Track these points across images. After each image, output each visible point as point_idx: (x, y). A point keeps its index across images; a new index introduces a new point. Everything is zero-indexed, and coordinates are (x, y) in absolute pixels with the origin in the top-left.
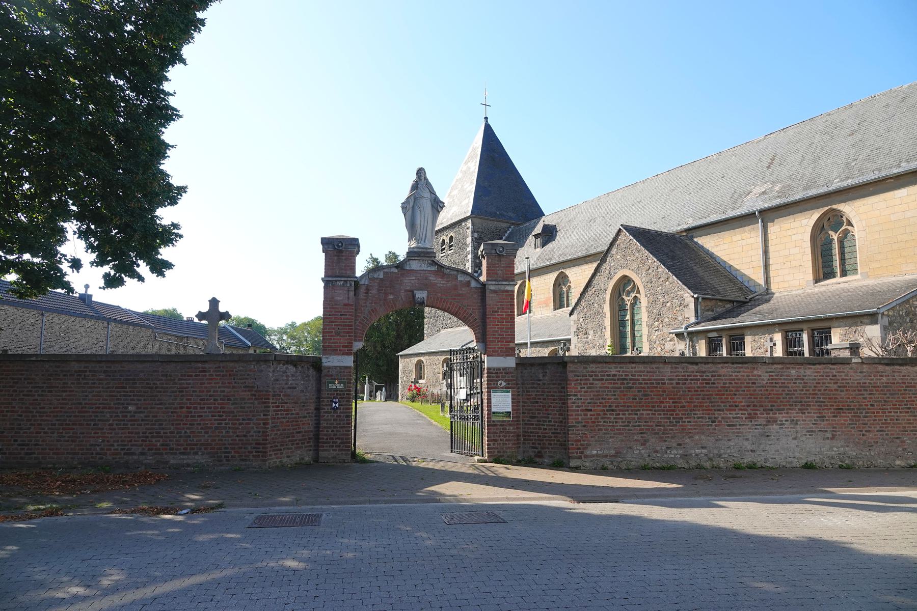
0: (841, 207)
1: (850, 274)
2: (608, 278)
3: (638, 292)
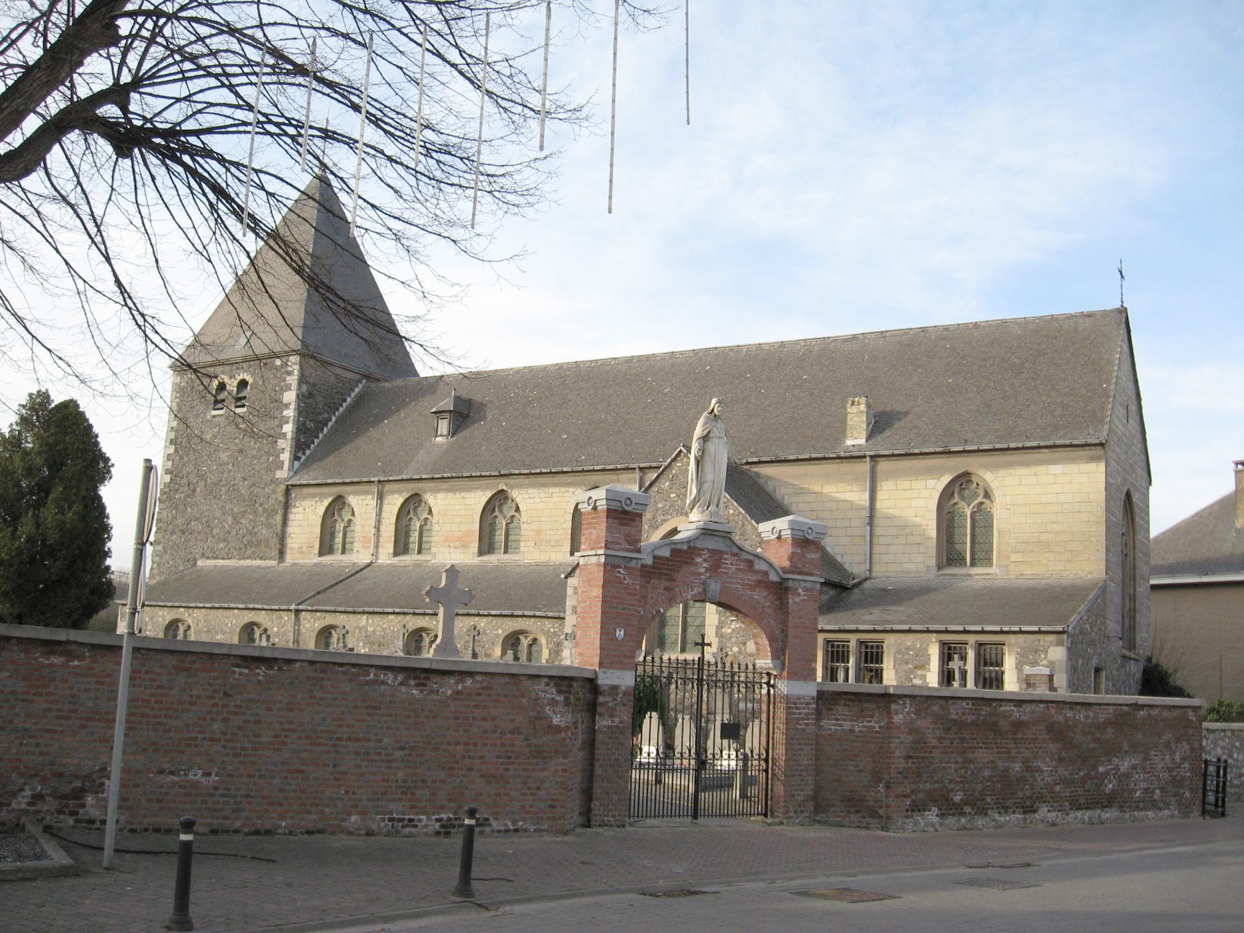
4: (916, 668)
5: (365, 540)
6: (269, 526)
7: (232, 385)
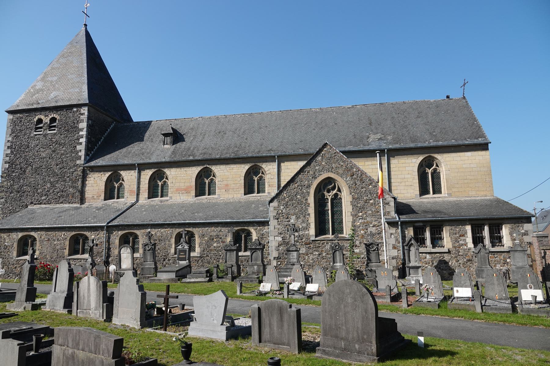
1: (437, 193)
2: (313, 177)
3: (339, 190)
4: (460, 236)
5: (131, 192)
6: (74, 187)
7: (46, 120)
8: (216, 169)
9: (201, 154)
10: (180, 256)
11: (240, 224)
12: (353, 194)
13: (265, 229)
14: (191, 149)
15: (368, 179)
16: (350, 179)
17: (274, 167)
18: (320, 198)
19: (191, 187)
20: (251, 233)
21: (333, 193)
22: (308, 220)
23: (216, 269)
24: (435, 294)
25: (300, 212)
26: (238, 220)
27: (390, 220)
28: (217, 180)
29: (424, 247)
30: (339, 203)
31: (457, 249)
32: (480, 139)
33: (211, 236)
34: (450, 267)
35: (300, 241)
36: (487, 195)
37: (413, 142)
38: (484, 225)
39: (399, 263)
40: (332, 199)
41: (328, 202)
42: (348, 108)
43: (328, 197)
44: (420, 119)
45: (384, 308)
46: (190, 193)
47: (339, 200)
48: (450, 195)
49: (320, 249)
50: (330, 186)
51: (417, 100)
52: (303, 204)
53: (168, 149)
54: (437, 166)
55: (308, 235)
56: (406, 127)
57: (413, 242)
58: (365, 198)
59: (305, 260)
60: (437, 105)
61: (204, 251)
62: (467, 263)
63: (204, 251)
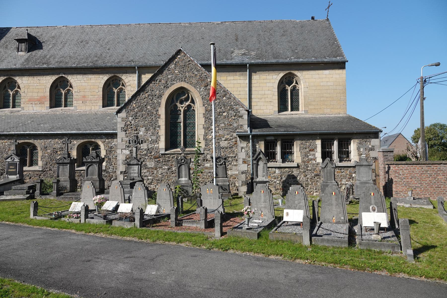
0: (296, 73)
1: (295, 110)
2: (164, 87)
3: (193, 102)
4: (310, 151)
8: (73, 79)
9: (57, 62)
10: (9, 170)
11: (87, 136)
12: (206, 105)
13: (114, 142)
14: (48, 57)
15: (222, 90)
16: (204, 90)
17: (134, 79)
18: (172, 110)
19: (45, 97)
20: (100, 146)
21: (186, 105)
22: (158, 133)
23: (39, 184)
24: (265, 215)
25: (150, 124)
26: (84, 132)
27: (242, 133)
28: (74, 91)
29: (274, 162)
30: (192, 115)
31: (306, 164)
32: (338, 58)
33: (54, 149)
34: (298, 182)
35: (149, 155)
36: (341, 113)
37: (275, 58)
38: (333, 140)
39: (249, 178)
40: (185, 112)
41: (181, 114)
42: (217, 24)
43: (181, 109)
44: (284, 37)
45: (187, 239)
46: (44, 103)
47: (192, 112)
48: (306, 112)
49: (170, 163)
50: (183, 97)
51: (284, 20)
52: (154, 116)
53: (22, 56)
54: (297, 83)
55: (158, 148)
56: (270, 44)
57: (261, 156)
58: (218, 110)
59: (153, 175)
60: (302, 25)
61: (46, 164)
62: (314, 178)
63: (46, 164)
